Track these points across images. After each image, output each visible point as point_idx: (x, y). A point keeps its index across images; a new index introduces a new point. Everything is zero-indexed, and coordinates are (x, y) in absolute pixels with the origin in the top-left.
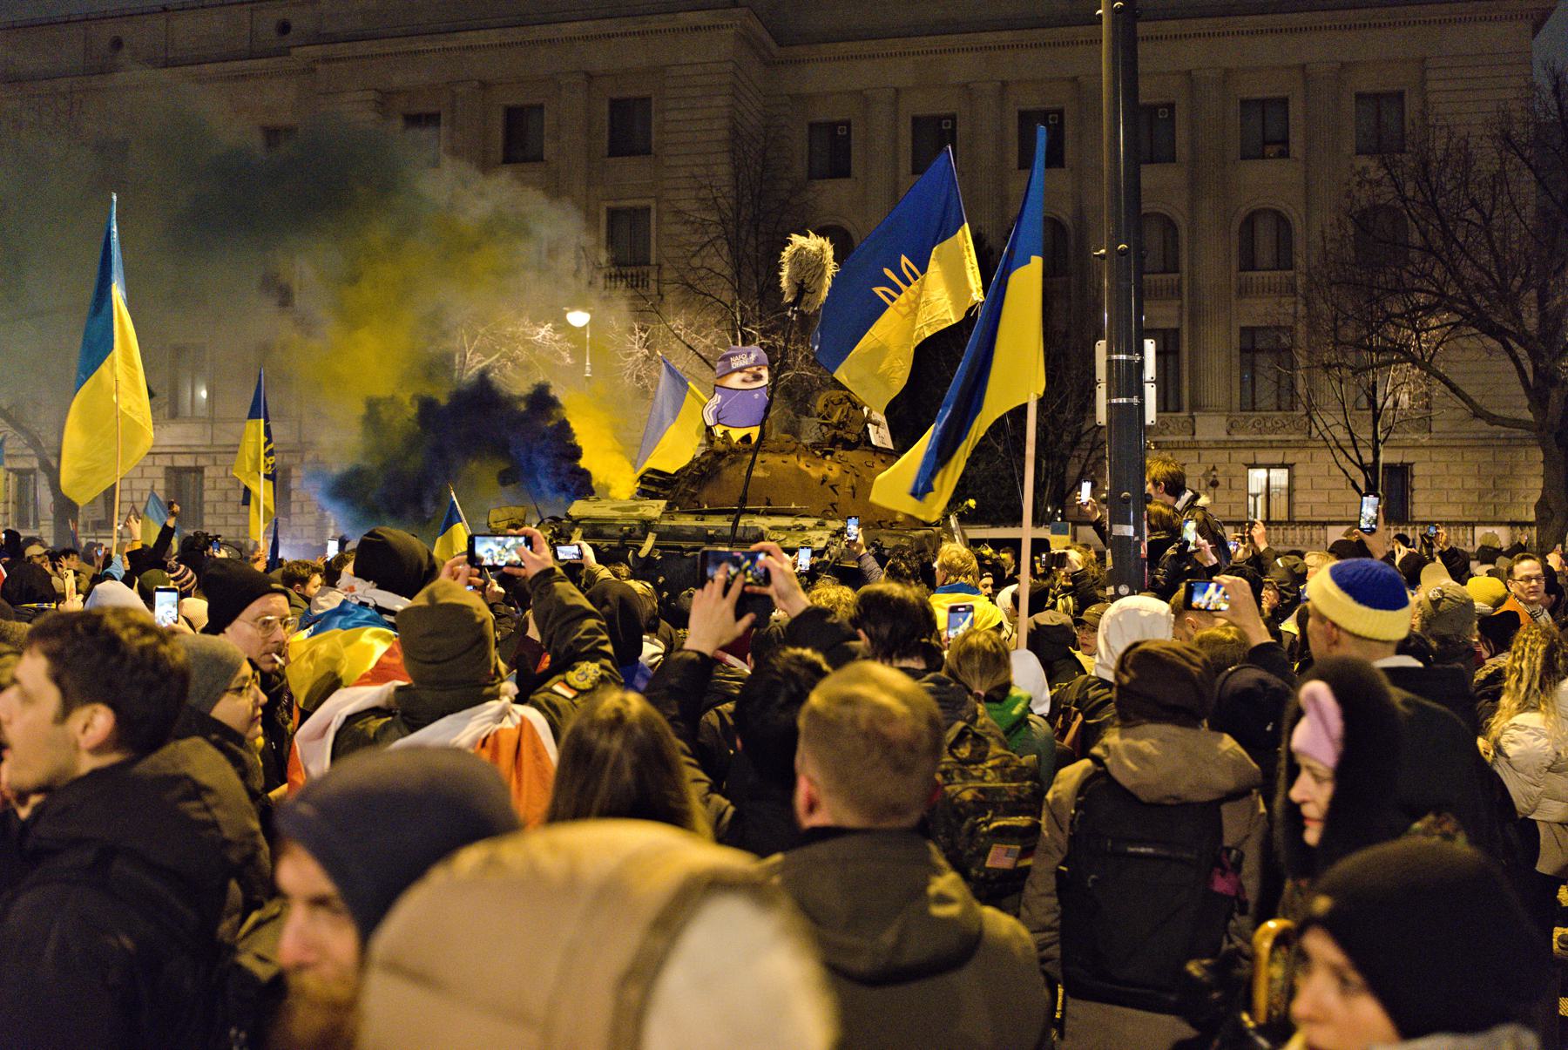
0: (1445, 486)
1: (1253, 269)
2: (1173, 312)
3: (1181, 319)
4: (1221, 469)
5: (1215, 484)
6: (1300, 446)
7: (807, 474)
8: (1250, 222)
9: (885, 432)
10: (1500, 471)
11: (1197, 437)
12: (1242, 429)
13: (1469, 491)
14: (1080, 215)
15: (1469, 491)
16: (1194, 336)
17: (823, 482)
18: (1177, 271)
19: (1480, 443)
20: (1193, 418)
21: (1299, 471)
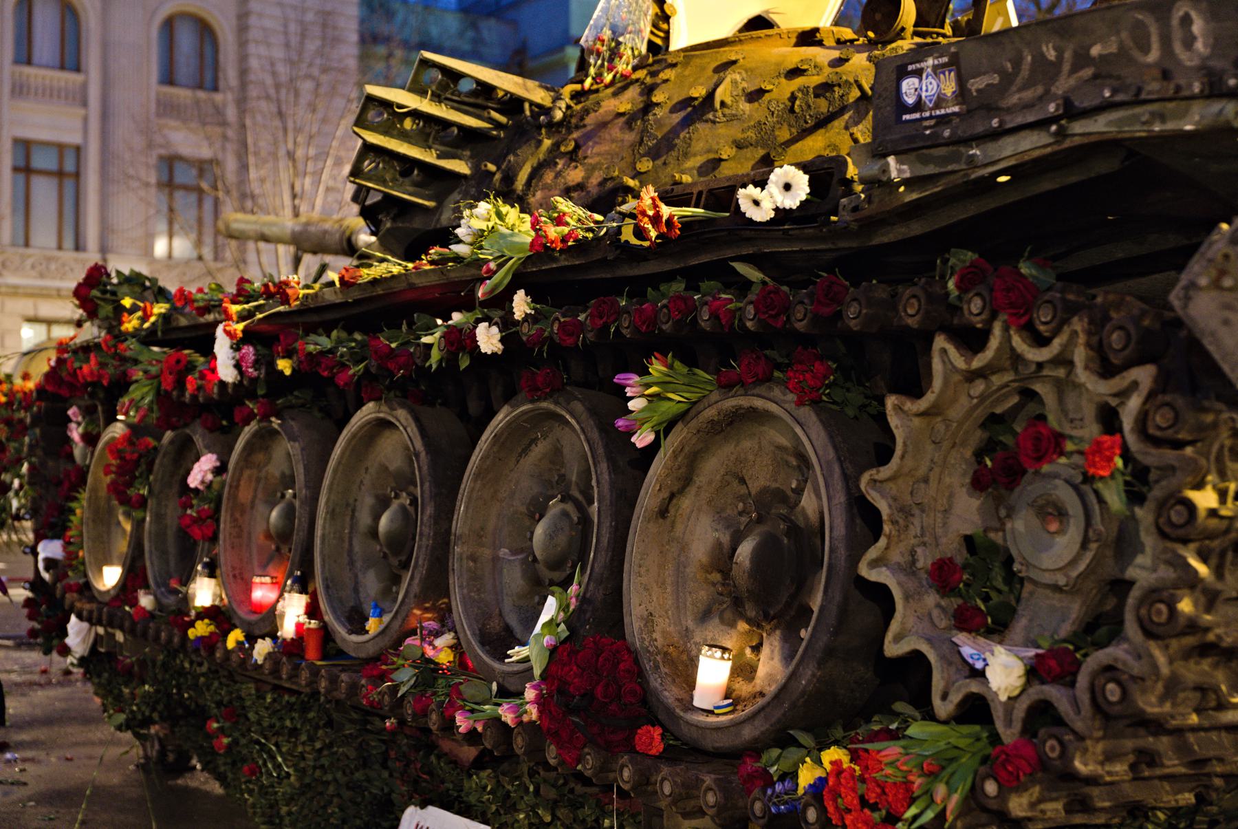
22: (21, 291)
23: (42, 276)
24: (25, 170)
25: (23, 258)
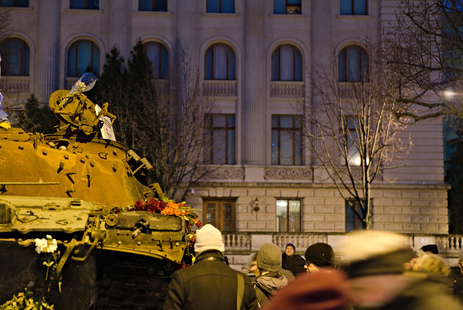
0: (392, 212)
1: (279, 79)
2: (233, 104)
3: (237, 108)
4: (261, 200)
5: (257, 209)
6: (307, 186)
7: (43, 161)
8: (278, 52)
9: (111, 131)
10: (422, 204)
11: (246, 180)
12: (272, 176)
13: (407, 216)
14: (177, 42)
15: (407, 216)
16: (244, 120)
17: (60, 169)
18: (234, 79)
19: (412, 187)
20: (244, 168)
21: (306, 202)
22: (273, 185)
23: (284, 178)
24: (277, 129)
25: (275, 170)
